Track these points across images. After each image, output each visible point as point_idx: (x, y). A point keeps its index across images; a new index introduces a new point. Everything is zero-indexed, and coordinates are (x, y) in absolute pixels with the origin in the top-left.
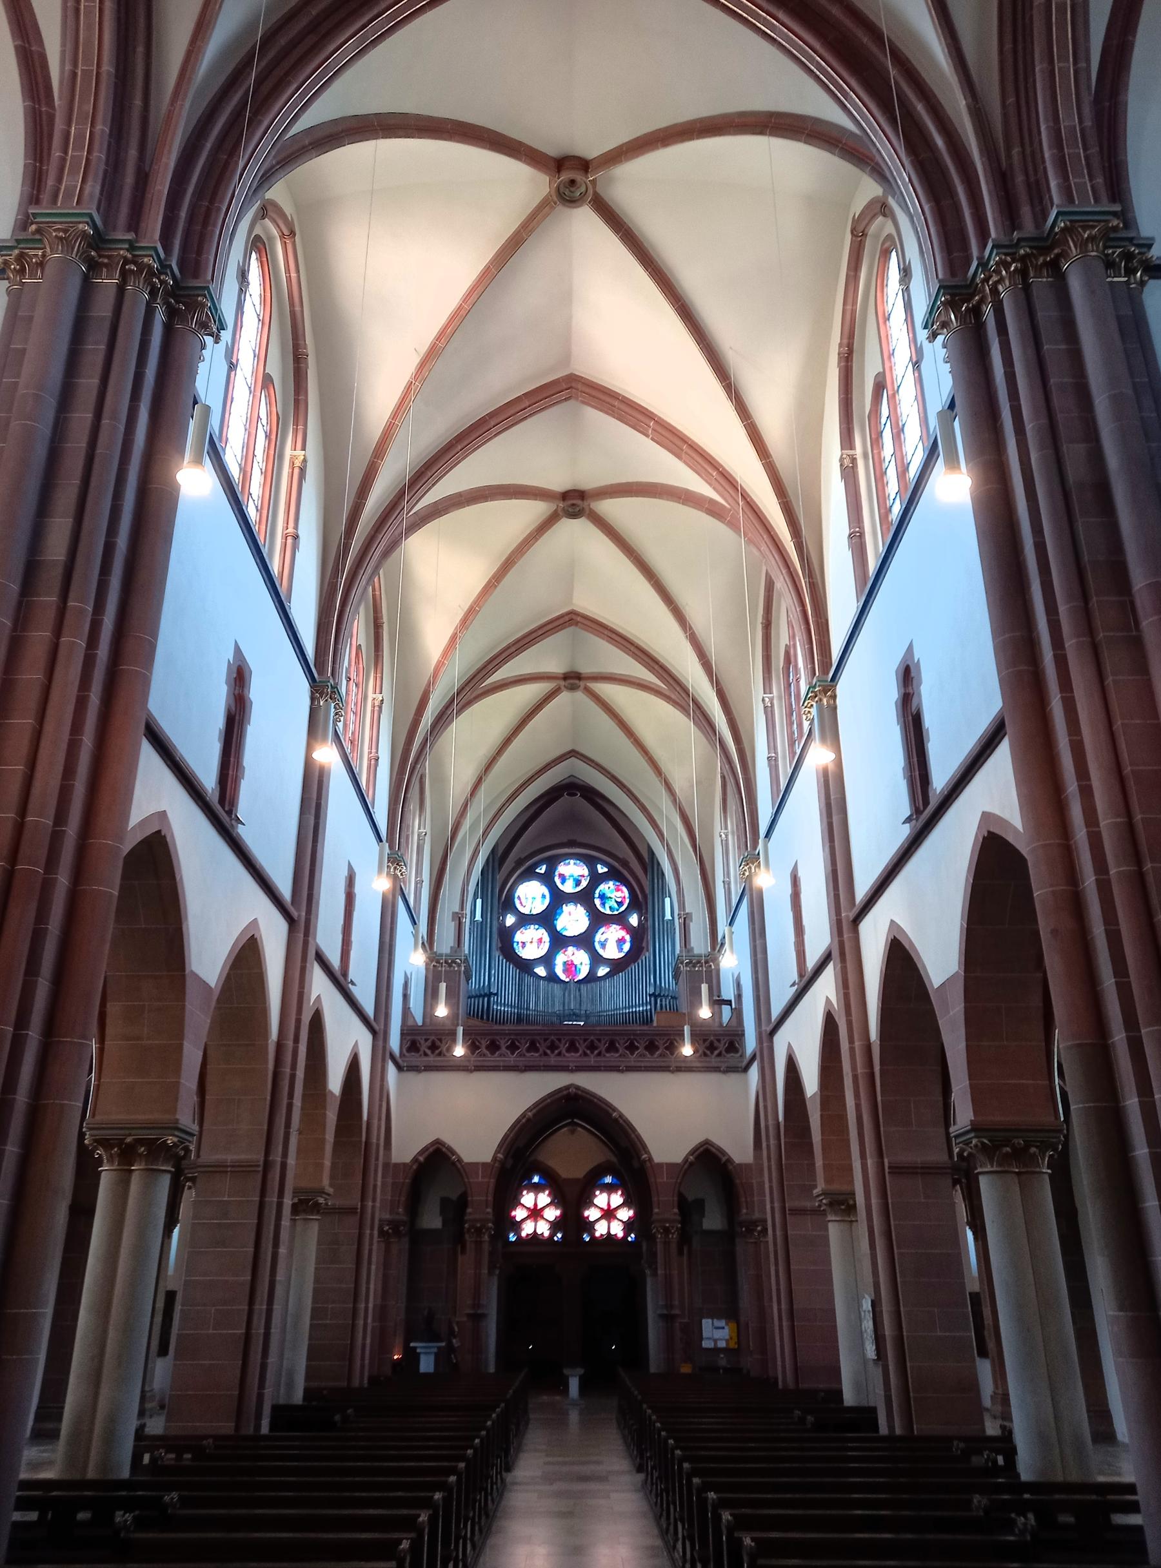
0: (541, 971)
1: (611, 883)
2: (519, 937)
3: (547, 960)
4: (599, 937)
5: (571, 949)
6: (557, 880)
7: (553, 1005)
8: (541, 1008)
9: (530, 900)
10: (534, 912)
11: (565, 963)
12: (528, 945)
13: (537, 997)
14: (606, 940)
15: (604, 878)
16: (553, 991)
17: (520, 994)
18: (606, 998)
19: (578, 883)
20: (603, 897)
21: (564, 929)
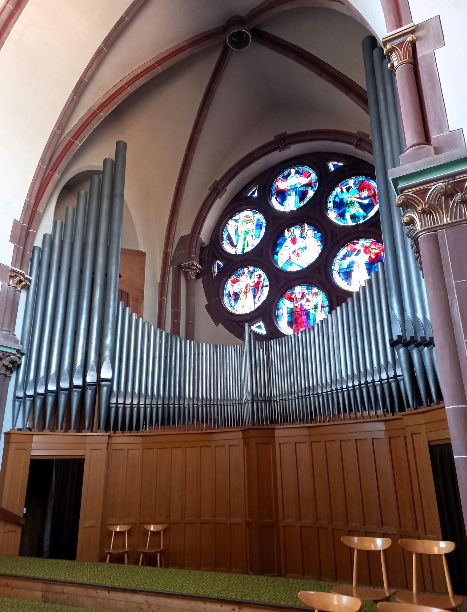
0: (260, 328)
1: (351, 182)
2: (230, 287)
3: (267, 313)
4: (338, 264)
5: (298, 290)
6: (275, 202)
7: (225, 387)
8: (203, 392)
9: (242, 237)
10: (248, 249)
11: (292, 313)
12: (241, 296)
13: (197, 373)
14: (350, 266)
15: (340, 177)
16: (223, 359)
17: (168, 371)
18: (315, 357)
19: (302, 196)
20: (340, 205)
21: (289, 262)
